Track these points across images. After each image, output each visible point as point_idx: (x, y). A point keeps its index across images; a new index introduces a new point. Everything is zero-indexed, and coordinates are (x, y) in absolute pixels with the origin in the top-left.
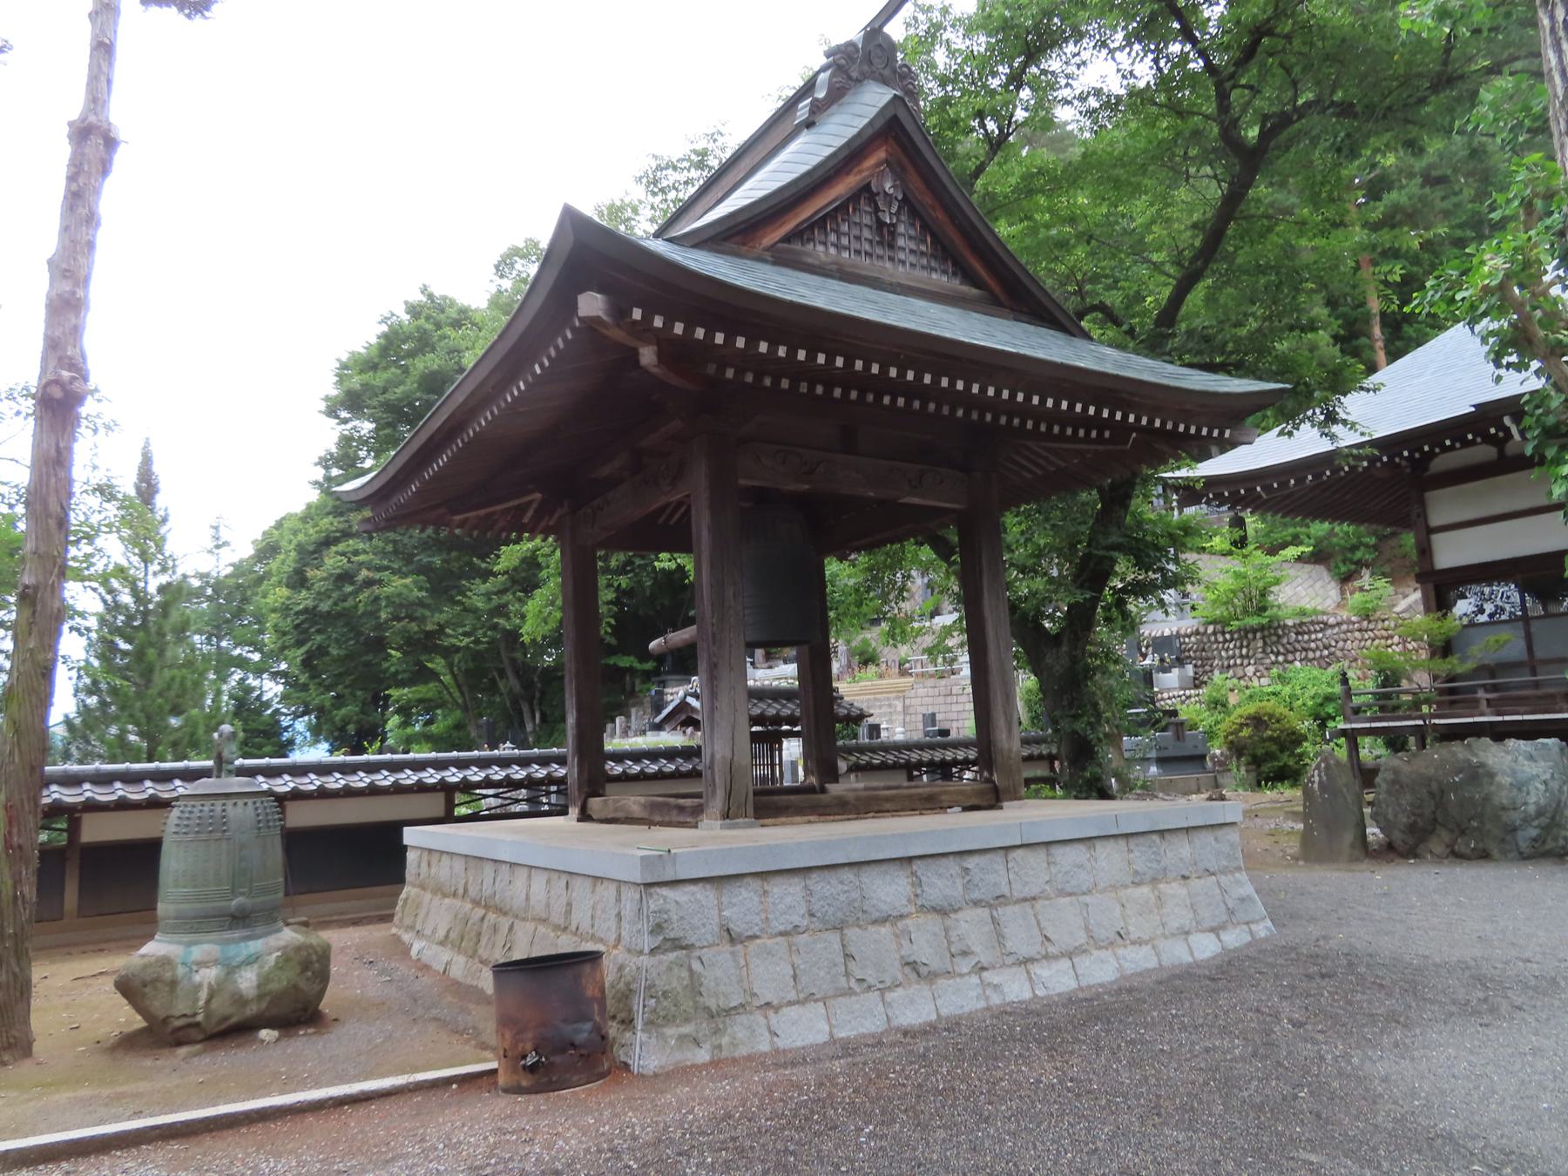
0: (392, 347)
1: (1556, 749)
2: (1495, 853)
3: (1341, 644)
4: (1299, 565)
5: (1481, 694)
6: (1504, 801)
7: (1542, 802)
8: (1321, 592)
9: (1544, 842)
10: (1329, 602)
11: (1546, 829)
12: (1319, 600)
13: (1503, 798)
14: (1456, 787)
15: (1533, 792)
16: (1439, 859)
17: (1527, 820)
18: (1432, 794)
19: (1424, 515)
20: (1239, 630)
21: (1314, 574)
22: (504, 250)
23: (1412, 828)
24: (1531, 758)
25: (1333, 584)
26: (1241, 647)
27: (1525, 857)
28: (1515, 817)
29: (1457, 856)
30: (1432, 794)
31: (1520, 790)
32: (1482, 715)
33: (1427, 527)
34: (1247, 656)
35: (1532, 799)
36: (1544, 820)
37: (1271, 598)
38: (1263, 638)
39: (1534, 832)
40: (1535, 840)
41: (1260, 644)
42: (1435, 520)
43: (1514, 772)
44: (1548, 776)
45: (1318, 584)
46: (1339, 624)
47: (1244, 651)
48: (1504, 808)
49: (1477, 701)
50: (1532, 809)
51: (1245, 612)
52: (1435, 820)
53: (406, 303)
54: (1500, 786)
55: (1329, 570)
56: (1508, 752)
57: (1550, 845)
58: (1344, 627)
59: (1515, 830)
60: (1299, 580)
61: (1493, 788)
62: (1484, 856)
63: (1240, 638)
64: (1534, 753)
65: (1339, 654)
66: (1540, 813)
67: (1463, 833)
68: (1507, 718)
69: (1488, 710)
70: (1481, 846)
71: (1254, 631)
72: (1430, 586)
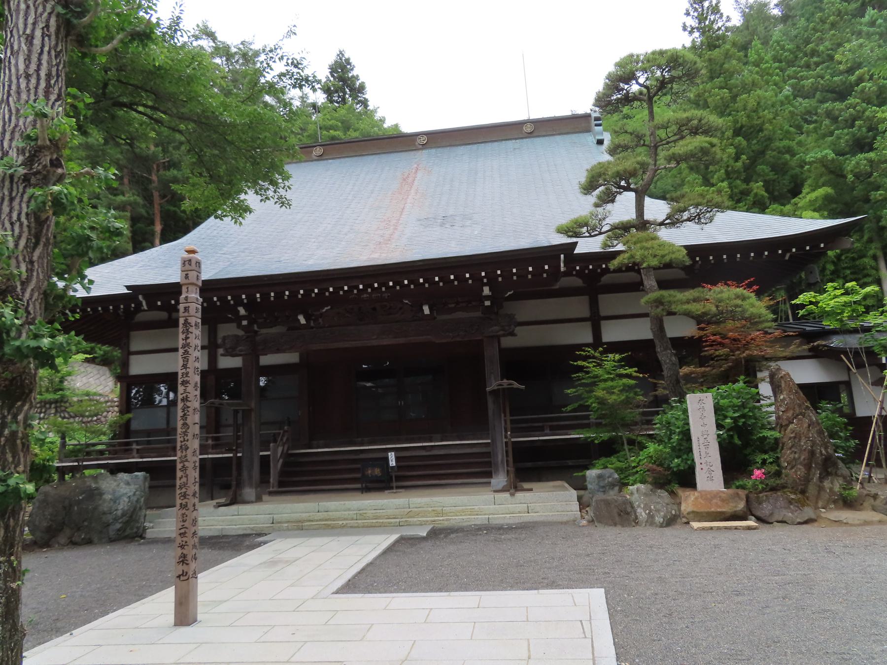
0: (596, 100)
1: (142, 478)
2: (96, 540)
3: (105, 414)
4: (86, 364)
5: (135, 446)
6: (105, 509)
7: (126, 508)
8: (103, 382)
9: (125, 531)
10: (107, 389)
11: (127, 523)
12: (101, 387)
13: (105, 507)
14: (79, 502)
15: (122, 503)
16: (62, 547)
17: (116, 520)
18: (64, 508)
19: (128, 345)
20: (40, 402)
21: (101, 372)
22: (610, 67)
23: (49, 530)
24: (128, 484)
25: (111, 379)
26: (40, 413)
27: (112, 541)
28: (110, 518)
29: (73, 544)
30: (64, 508)
31: (115, 502)
32: (133, 458)
33: (129, 351)
34: (43, 418)
35: (121, 507)
36: (125, 519)
37: (66, 383)
38: (56, 408)
39: (118, 526)
40: (119, 530)
41: (53, 411)
42: (134, 347)
43: (114, 492)
44: (131, 494)
45: (103, 378)
46: (107, 402)
47: (42, 415)
48: (104, 513)
49: (131, 450)
50: (119, 513)
51: (47, 391)
52: (64, 523)
53: (341, 53)
54: (105, 500)
55: (110, 370)
56: (115, 481)
57: (128, 532)
58: (109, 404)
59: (108, 525)
60: (92, 375)
61: (100, 502)
62: (89, 542)
63: (41, 407)
64: (130, 480)
65: (103, 419)
66: (123, 515)
67: (79, 529)
68: (145, 460)
69: (136, 455)
70: (88, 537)
71: (50, 403)
72: (125, 384)
